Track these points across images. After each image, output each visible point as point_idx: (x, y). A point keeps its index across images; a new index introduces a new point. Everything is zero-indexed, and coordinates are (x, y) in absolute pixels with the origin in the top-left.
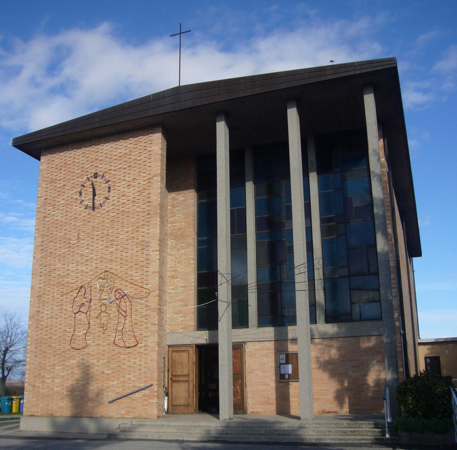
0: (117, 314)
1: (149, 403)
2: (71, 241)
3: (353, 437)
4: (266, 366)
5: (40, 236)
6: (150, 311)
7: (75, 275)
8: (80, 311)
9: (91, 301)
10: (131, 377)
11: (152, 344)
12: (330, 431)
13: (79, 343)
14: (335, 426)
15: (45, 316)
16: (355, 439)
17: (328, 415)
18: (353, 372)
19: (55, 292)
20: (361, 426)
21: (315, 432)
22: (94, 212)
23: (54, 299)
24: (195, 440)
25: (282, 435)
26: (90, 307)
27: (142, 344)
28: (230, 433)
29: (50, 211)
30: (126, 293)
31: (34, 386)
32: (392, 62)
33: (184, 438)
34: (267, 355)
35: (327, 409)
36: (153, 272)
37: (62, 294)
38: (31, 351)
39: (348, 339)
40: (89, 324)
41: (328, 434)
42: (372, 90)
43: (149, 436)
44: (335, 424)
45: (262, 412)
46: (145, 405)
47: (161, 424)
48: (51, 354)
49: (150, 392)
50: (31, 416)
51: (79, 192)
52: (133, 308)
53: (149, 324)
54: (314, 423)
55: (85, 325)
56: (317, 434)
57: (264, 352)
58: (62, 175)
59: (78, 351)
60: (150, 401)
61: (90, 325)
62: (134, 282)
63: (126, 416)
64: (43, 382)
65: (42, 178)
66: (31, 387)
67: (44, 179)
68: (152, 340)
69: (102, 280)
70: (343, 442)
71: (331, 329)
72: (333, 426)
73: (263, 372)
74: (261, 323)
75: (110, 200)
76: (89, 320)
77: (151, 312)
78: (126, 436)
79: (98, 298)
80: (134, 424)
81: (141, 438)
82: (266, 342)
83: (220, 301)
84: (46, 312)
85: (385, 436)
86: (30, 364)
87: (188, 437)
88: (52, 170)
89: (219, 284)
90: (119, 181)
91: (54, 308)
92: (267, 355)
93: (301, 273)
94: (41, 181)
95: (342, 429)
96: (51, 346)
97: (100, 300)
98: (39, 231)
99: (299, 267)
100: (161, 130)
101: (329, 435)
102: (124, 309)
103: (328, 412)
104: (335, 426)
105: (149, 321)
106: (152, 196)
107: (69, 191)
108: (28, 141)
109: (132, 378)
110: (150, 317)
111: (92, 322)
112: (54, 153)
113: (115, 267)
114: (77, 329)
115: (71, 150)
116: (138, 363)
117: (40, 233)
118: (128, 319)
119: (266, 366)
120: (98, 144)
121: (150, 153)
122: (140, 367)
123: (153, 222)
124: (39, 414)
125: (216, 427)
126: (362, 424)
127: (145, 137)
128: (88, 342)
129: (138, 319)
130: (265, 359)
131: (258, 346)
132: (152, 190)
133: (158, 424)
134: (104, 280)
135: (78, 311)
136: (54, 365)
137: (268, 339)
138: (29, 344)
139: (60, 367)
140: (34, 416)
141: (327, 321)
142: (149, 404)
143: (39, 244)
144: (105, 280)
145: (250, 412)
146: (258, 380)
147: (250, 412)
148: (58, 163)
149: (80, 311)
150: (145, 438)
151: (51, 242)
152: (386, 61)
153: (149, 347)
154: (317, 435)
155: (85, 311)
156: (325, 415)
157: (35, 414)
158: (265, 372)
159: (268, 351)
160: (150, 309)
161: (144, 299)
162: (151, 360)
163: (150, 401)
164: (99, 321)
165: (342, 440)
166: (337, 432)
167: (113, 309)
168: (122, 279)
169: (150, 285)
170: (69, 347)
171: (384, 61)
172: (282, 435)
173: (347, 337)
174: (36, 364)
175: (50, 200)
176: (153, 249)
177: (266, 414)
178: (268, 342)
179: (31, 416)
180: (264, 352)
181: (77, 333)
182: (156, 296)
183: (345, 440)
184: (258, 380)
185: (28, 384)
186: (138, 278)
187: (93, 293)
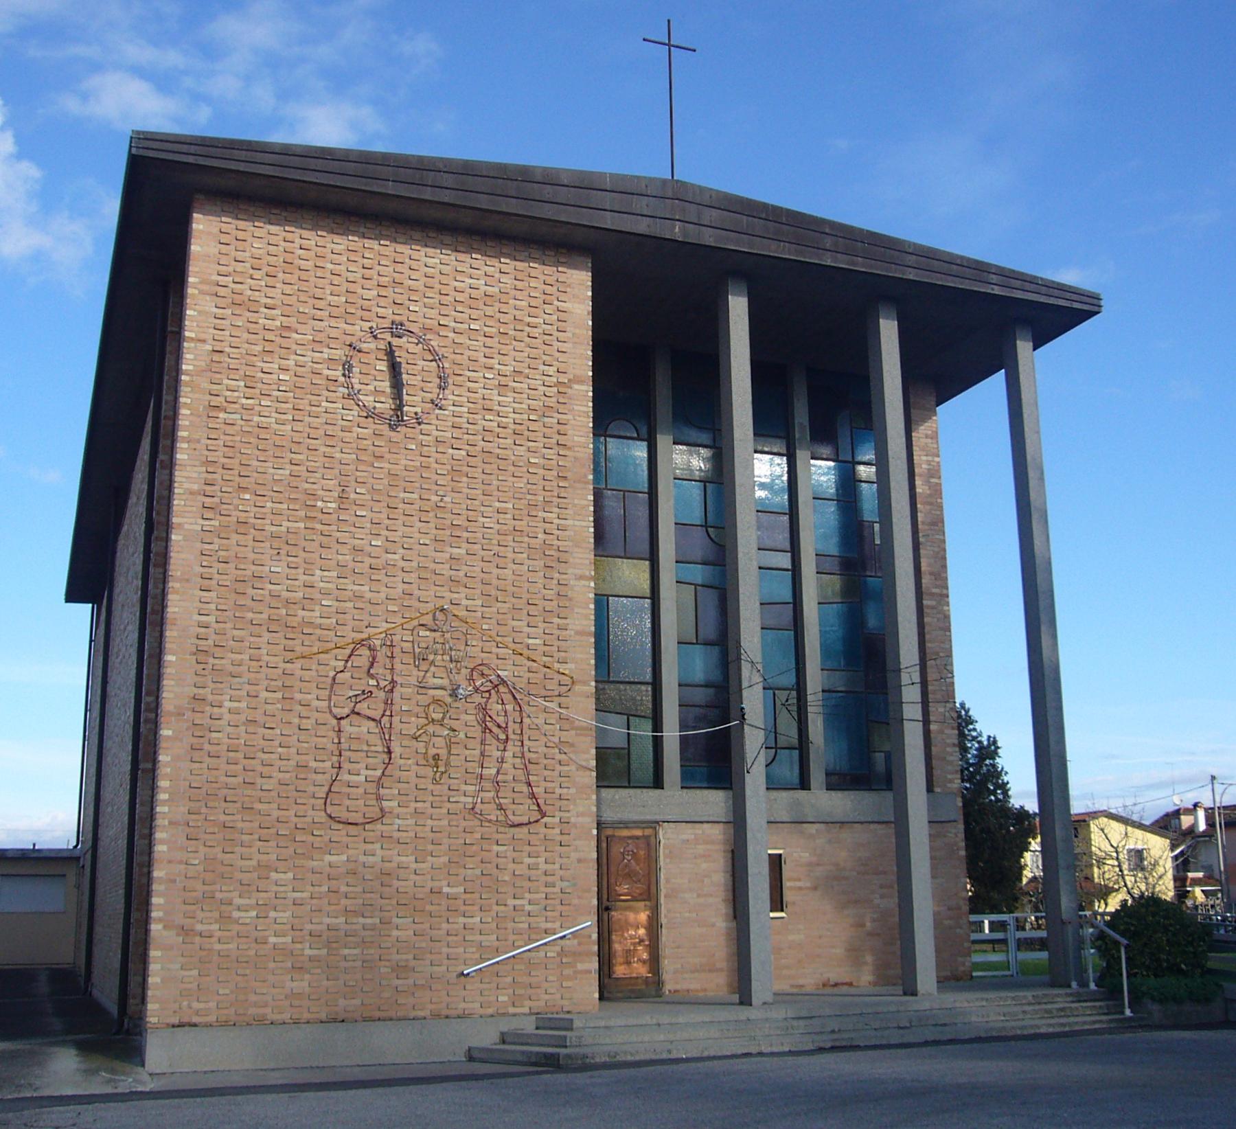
0: (476, 732)
1: (575, 972)
2: (316, 500)
3: (1062, 1020)
4: (706, 880)
5: (197, 463)
6: (573, 732)
7: (336, 604)
8: (358, 714)
9: (393, 687)
10: (524, 905)
11: (580, 819)
12: (1024, 1012)
13: (355, 806)
14: (1014, 1002)
15: (227, 717)
16: (1085, 1023)
17: (836, 990)
18: (882, 897)
19: (263, 646)
20: (1055, 1000)
21: (999, 1014)
22: (393, 434)
23: (261, 667)
24: (787, 1049)
25: (941, 1025)
26: (388, 703)
27: (553, 817)
28: (839, 1030)
29: (236, 394)
30: (506, 676)
31: (184, 931)
32: (1095, 302)
33: (763, 1048)
34: (709, 856)
35: (834, 976)
36: (578, 633)
37: (289, 655)
38: (171, 823)
39: (872, 826)
40: (390, 752)
41: (1021, 1016)
42: (1030, 336)
43: (675, 1052)
44: (1013, 998)
45: (697, 991)
46: (568, 978)
47: (654, 1021)
48: (251, 834)
49: (579, 944)
50: (181, 1025)
51: (342, 363)
52: (526, 721)
53: (573, 768)
54: (977, 999)
55: (376, 755)
56: (1003, 1018)
57: (701, 848)
58: (276, 293)
59: (353, 830)
60: (580, 966)
61: (393, 755)
62: (525, 652)
63: (512, 1010)
64: (224, 919)
65: (201, 283)
66: (178, 935)
67: (206, 288)
68: (581, 809)
69: (428, 633)
70: (1067, 1029)
71: (840, 803)
72: (1009, 1003)
73: (699, 896)
74: (689, 780)
75: (446, 412)
76: (390, 740)
77: (577, 735)
78: (615, 1057)
79: (413, 681)
80: (581, 1025)
81: (654, 1057)
82: (706, 825)
83: (750, 725)
84: (227, 704)
85: (1123, 1013)
86: (170, 862)
87: (771, 1045)
88: (239, 267)
89: (745, 684)
90: (472, 366)
91: (261, 696)
92: (709, 856)
93: (913, 684)
94: (197, 292)
95: (1044, 1006)
96: (252, 808)
97: (422, 687)
98: (193, 446)
99: (909, 670)
100: (590, 265)
101: (1023, 1019)
102: (501, 720)
103: (836, 985)
104: (1014, 1002)
105: (571, 759)
106: (568, 429)
107: (306, 350)
108: (191, 159)
109: (528, 908)
110: (572, 749)
111: (397, 750)
112: (245, 217)
113: (467, 601)
114: (346, 766)
115: (310, 227)
116: (543, 867)
117: (197, 453)
118: (512, 748)
119: (706, 880)
120: (401, 240)
121: (562, 316)
122: (549, 879)
123: (576, 502)
124: (212, 1018)
125: (786, 1019)
126: (1058, 995)
127: (549, 270)
128: (385, 804)
129: (540, 751)
130: (704, 866)
131: (688, 832)
132: (569, 417)
133: (644, 1022)
134: (433, 634)
135: (346, 711)
136: (264, 869)
137: (711, 819)
138: (166, 801)
139: (290, 875)
140: (195, 1025)
141: (830, 787)
142: (579, 976)
143: (195, 487)
144: (438, 634)
145: (670, 991)
146: (687, 915)
147: (670, 991)
148: (261, 251)
149: (358, 714)
150: (665, 1056)
151: (245, 489)
152: (1088, 296)
153: (575, 825)
154: (1002, 1021)
155: (376, 714)
156: (829, 990)
157: (195, 1019)
158: (705, 895)
159: (709, 847)
160: (577, 729)
161: (557, 700)
162: (579, 861)
163: (580, 966)
164: (421, 747)
165: (1063, 1025)
166: (1036, 1012)
167: (464, 717)
168: (491, 637)
169: (571, 666)
170: (321, 817)
171: (1083, 295)
172: (941, 1025)
173: (873, 822)
174: (199, 864)
175: (237, 361)
176: (578, 572)
177: (708, 993)
178: (710, 825)
179: (181, 1025)
180: (701, 848)
181: (345, 777)
182: (588, 697)
183: (1069, 1024)
184: (687, 915)
185: (165, 927)
186: (537, 641)
187: (398, 666)
